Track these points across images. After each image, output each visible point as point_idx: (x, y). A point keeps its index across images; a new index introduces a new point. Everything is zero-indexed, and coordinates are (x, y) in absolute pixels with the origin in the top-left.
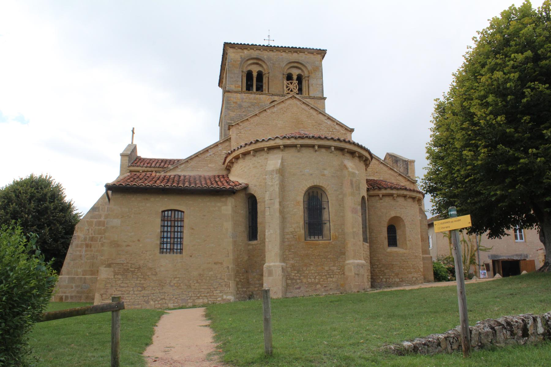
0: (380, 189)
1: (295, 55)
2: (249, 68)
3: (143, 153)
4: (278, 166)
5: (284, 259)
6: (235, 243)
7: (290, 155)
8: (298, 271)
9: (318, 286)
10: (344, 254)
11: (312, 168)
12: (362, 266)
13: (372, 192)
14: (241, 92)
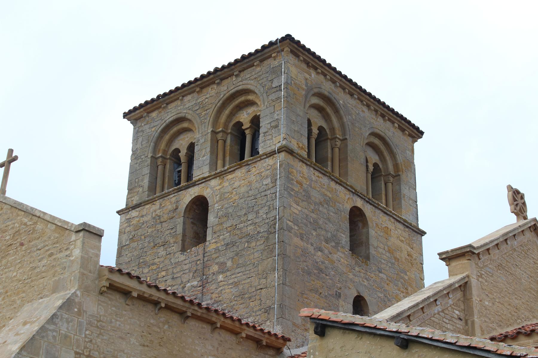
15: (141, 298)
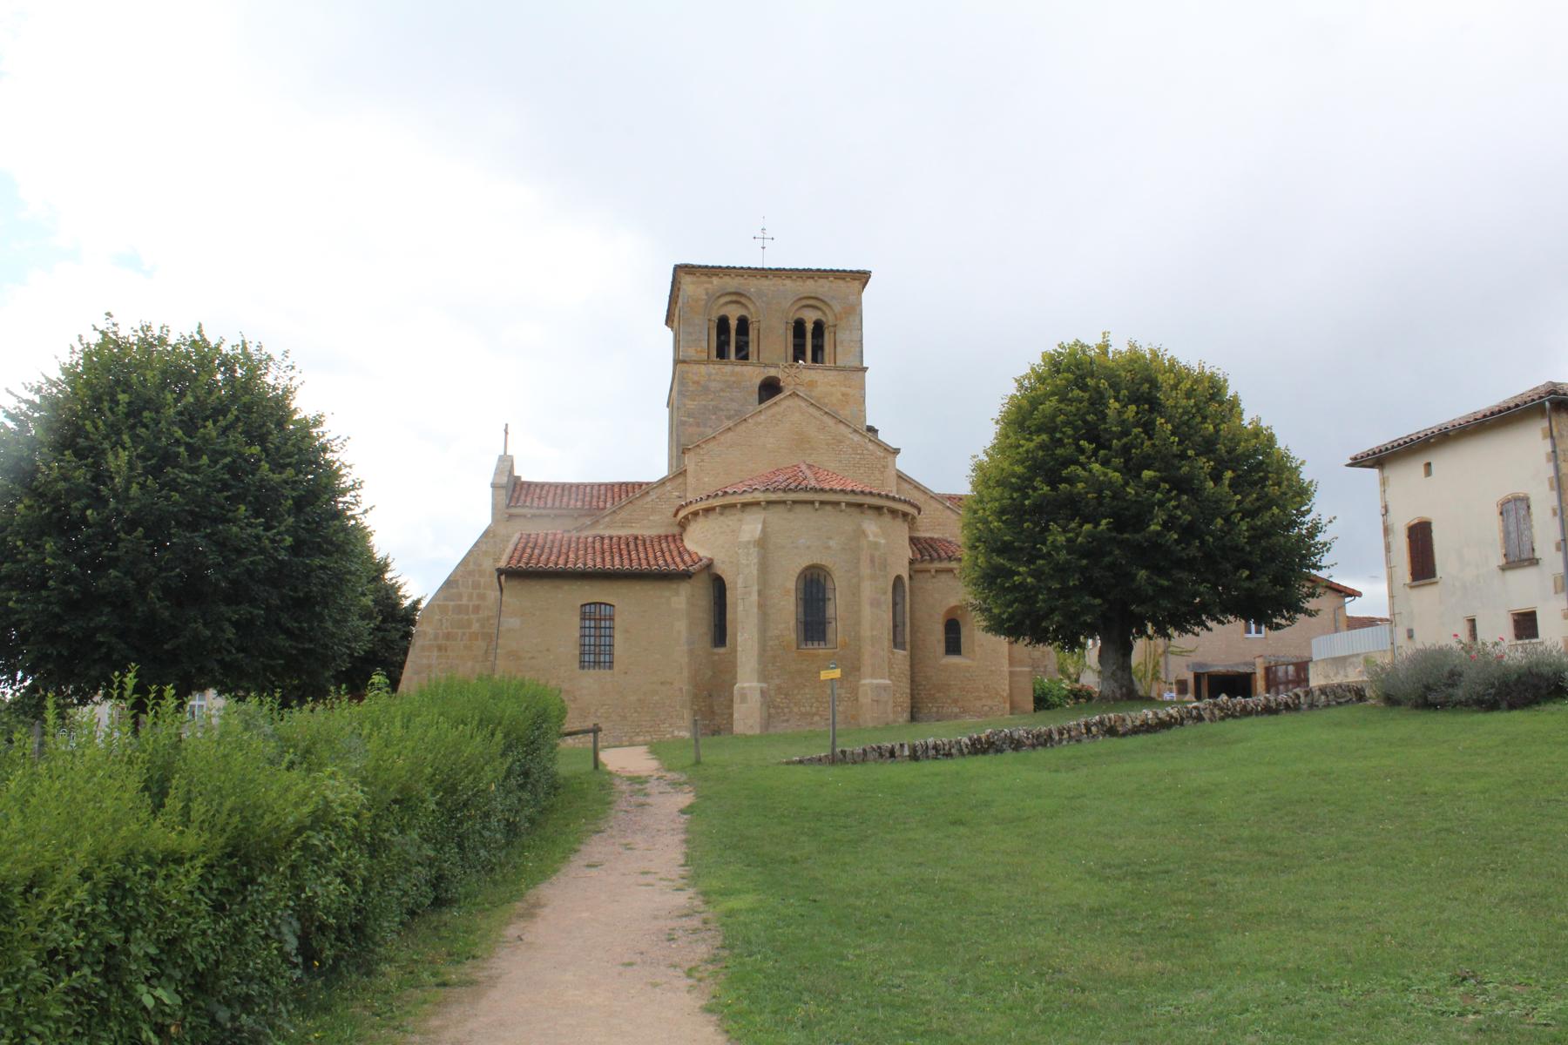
0: (932, 560)
1: (810, 283)
2: (722, 312)
3: (526, 473)
4: (758, 534)
5: (764, 676)
6: (691, 652)
7: (777, 517)
8: (786, 695)
9: (816, 718)
10: (859, 669)
11: (807, 540)
12: (885, 688)
13: (918, 566)
14: (708, 361)
15: (534, 516)
